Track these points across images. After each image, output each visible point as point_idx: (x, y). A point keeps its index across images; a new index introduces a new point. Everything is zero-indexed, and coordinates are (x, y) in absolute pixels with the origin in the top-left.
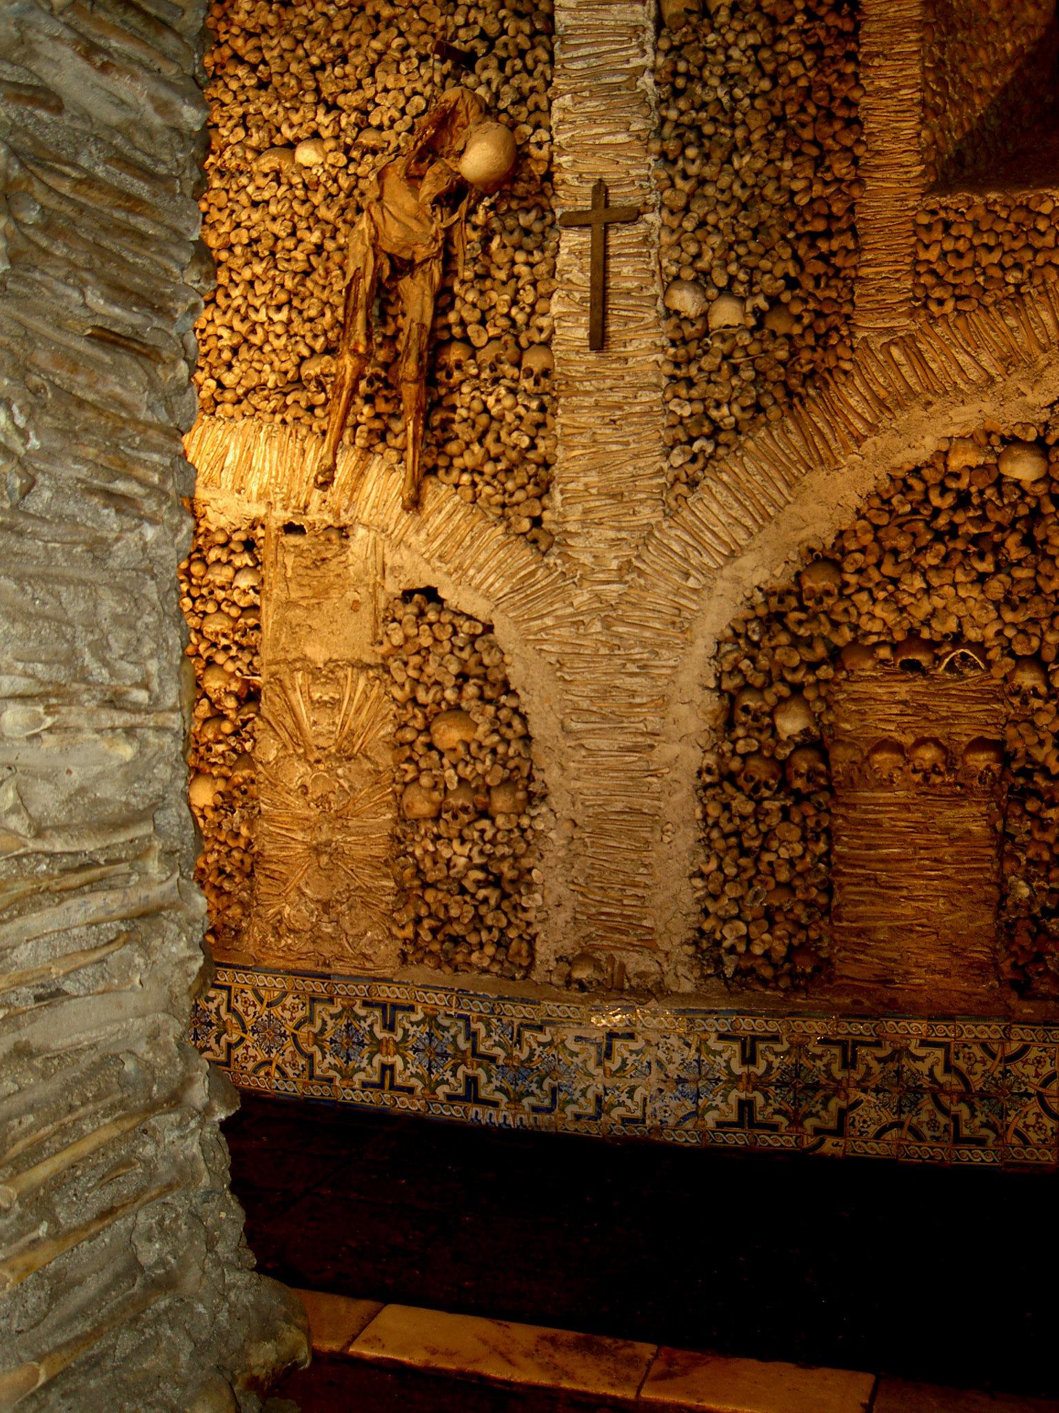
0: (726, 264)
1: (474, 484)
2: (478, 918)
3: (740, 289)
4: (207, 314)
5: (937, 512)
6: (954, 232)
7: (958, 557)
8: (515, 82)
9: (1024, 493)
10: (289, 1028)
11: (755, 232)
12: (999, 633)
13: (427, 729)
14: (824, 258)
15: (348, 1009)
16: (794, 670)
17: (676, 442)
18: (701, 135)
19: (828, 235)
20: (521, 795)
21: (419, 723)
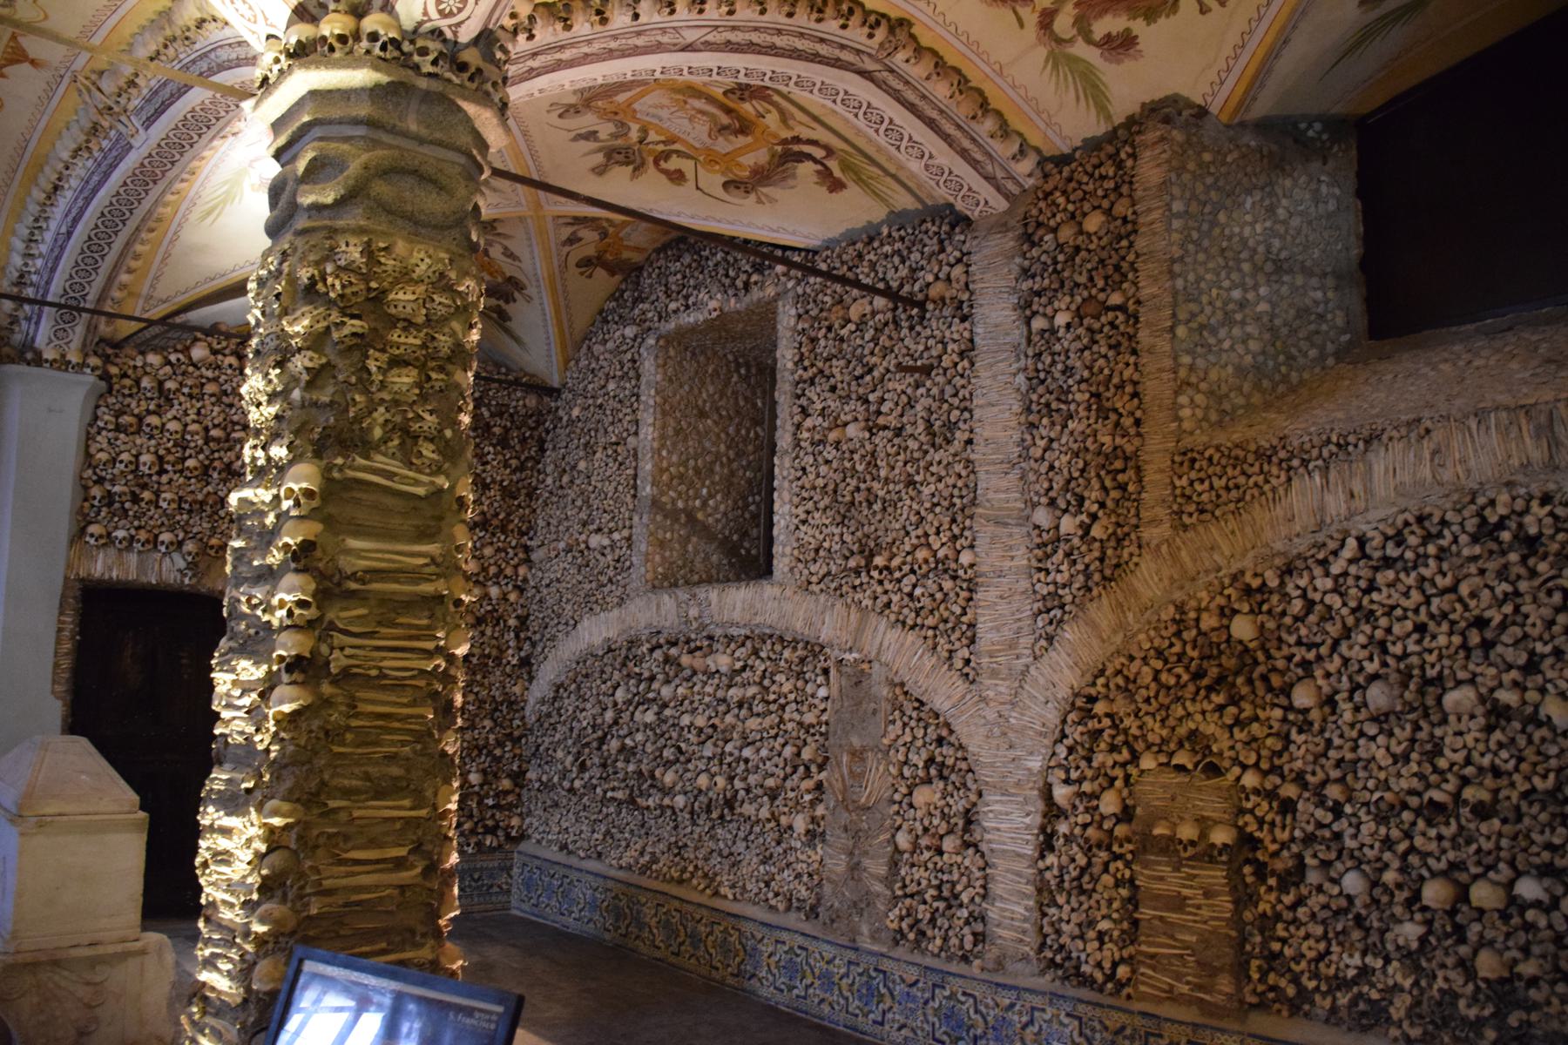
1: (935, 636)
2: (932, 921)
3: (1072, 509)
4: (803, 528)
5: (1192, 659)
6: (1197, 466)
7: (1203, 693)
9: (1246, 650)
10: (836, 979)
11: (1083, 471)
12: (1232, 748)
13: (910, 794)
14: (1122, 487)
15: (866, 971)
16: (1113, 767)
17: (1040, 612)
19: (1123, 471)
20: (958, 842)
21: (904, 790)
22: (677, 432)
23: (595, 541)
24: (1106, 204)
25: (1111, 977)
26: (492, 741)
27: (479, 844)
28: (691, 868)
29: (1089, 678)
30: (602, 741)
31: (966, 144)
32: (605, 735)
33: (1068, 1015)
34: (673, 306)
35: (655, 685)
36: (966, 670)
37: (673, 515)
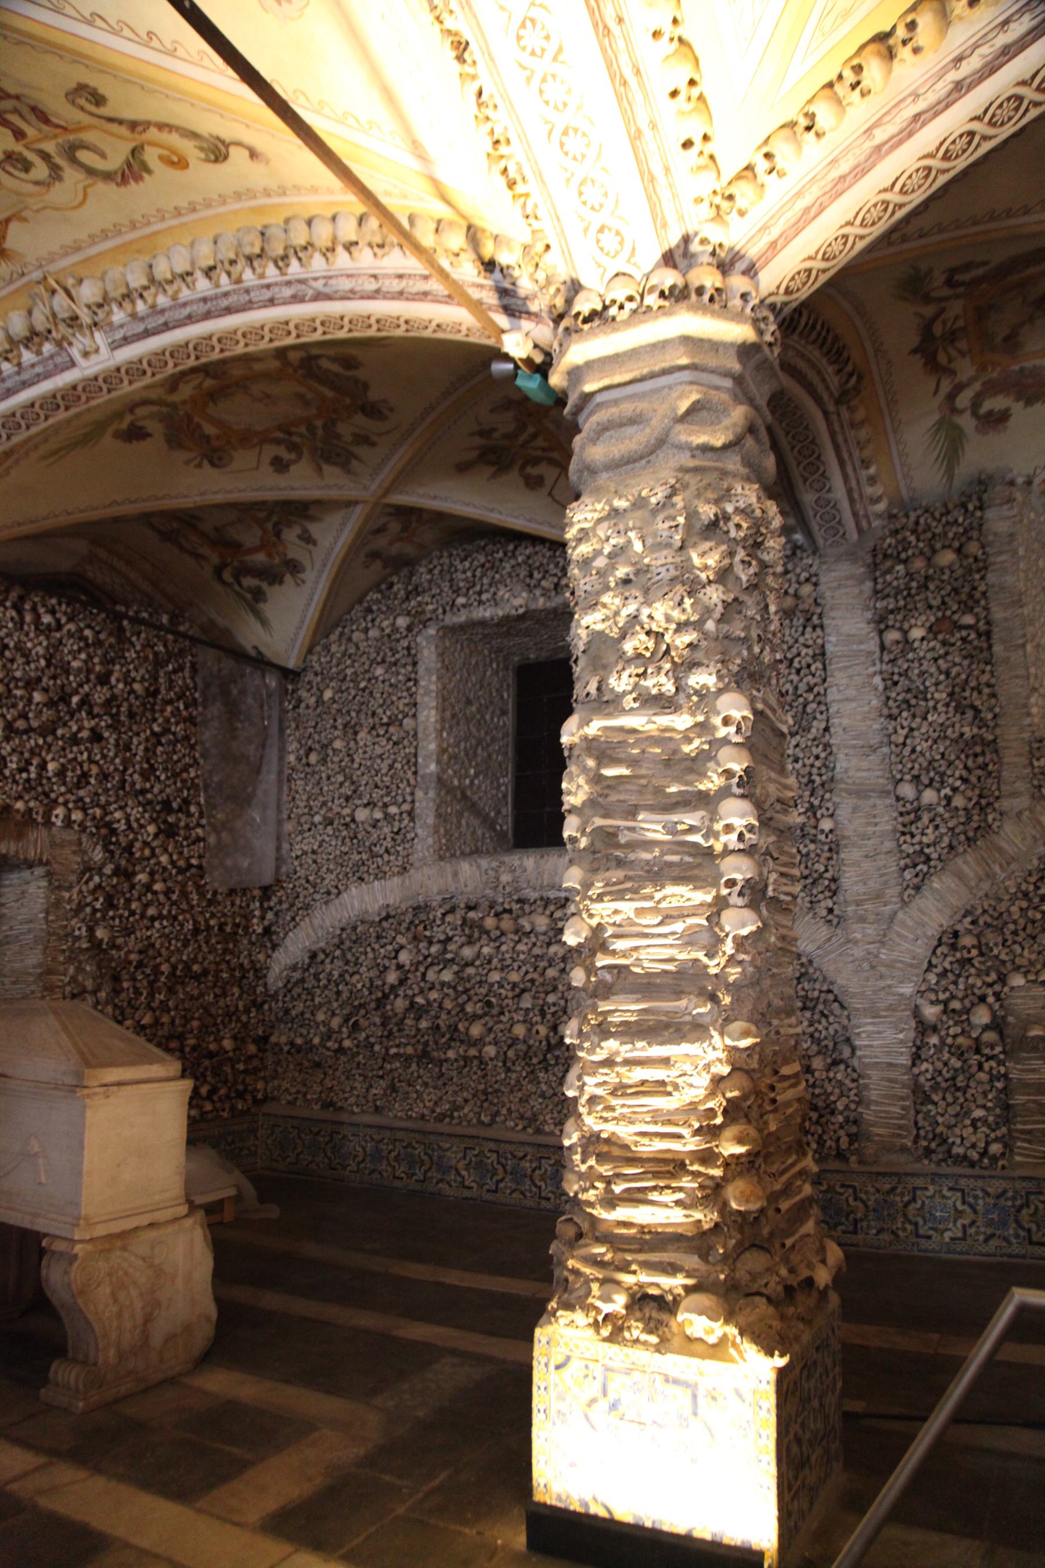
0: (928, 772)
3: (936, 785)
8: (805, 680)
17: (906, 867)
18: (909, 706)
22: (454, 716)
23: (362, 815)
24: (956, 544)
25: (984, 1153)
26: (241, 1008)
27: (233, 1108)
28: (504, 1111)
29: (958, 917)
30: (380, 1003)
31: (854, 483)
32: (385, 996)
33: (950, 1189)
34: (461, 600)
35: (451, 947)
36: (830, 917)
37: (450, 790)
